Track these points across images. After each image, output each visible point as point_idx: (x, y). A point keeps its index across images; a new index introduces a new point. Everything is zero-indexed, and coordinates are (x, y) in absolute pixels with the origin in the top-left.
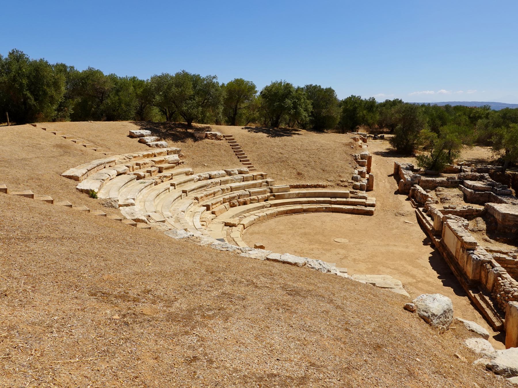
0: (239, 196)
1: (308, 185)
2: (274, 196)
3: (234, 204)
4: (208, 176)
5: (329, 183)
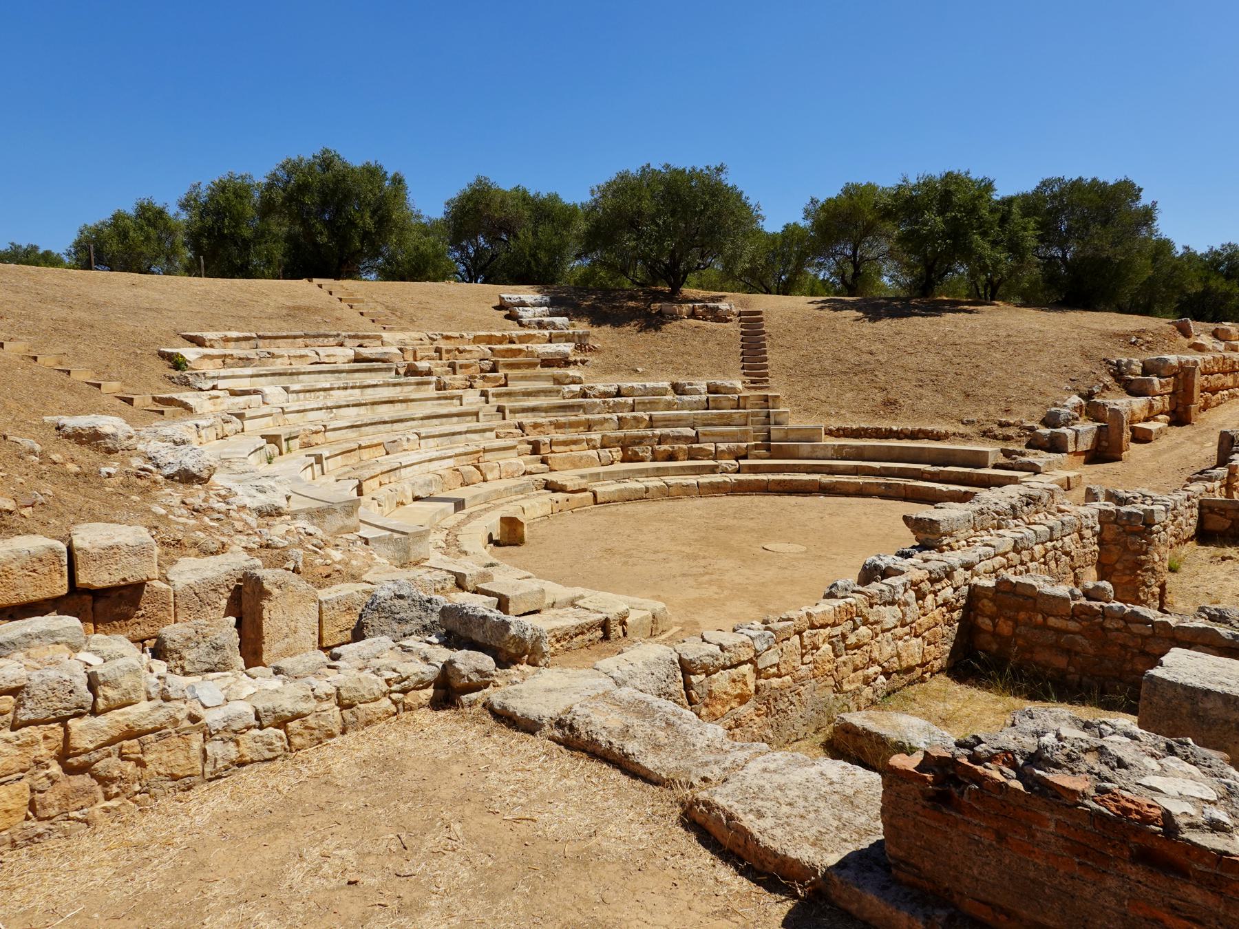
0: (662, 440)
1: (891, 430)
2: (768, 448)
4: (613, 389)
5: (962, 429)
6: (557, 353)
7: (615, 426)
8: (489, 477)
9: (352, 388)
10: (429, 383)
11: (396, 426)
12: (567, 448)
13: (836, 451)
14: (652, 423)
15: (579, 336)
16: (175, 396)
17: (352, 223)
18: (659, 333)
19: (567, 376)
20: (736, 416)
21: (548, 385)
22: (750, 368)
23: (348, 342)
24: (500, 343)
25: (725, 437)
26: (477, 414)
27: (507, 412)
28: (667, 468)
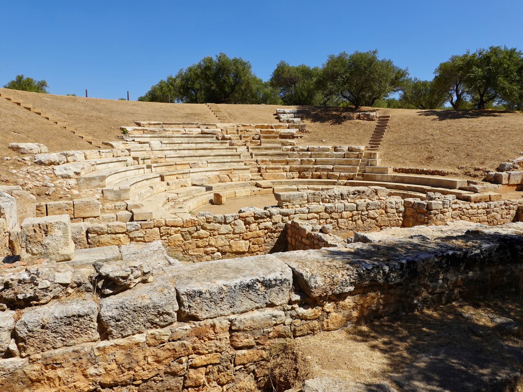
0: (317, 170)
1: (423, 170)
2: (363, 176)
3: (304, 175)
4: (306, 148)
5: (457, 171)
6: (289, 133)
7: (300, 163)
8: (233, 180)
10: (226, 143)
11: (201, 158)
12: (273, 171)
13: (392, 178)
14: (316, 163)
15: (301, 126)
16: (110, 142)
17: (224, 81)
18: (340, 125)
19: (288, 142)
20: (354, 161)
21: (279, 145)
22: (373, 141)
23: (201, 126)
24: (267, 128)
25: (345, 170)
26: (240, 155)
27: (253, 155)
28: (313, 182)
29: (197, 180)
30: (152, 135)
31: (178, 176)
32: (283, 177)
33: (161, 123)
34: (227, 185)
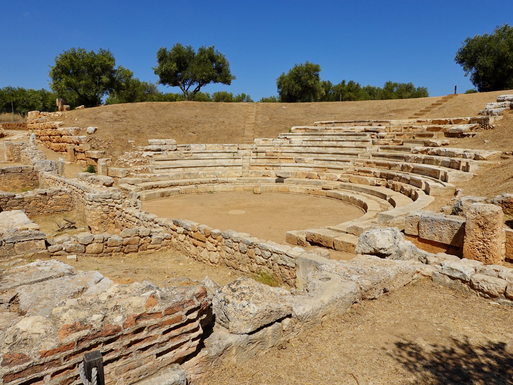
6: (457, 130)
7: (400, 169)
9: (333, 141)
12: (365, 174)
19: (431, 142)
23: (374, 124)
26: (357, 155)
29: (282, 173)
30: (303, 134)
31: (267, 167)
32: (366, 182)
33: (333, 121)
34: (300, 181)
